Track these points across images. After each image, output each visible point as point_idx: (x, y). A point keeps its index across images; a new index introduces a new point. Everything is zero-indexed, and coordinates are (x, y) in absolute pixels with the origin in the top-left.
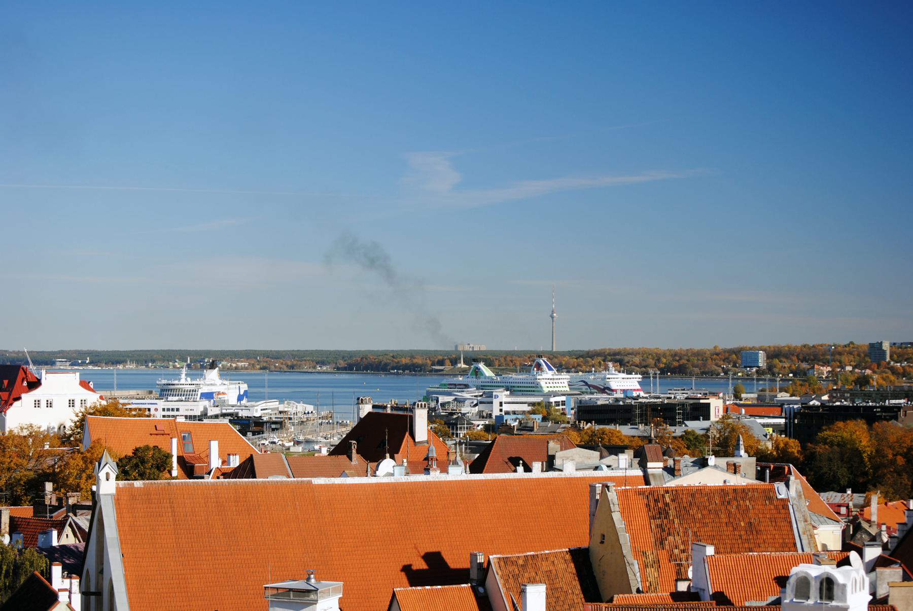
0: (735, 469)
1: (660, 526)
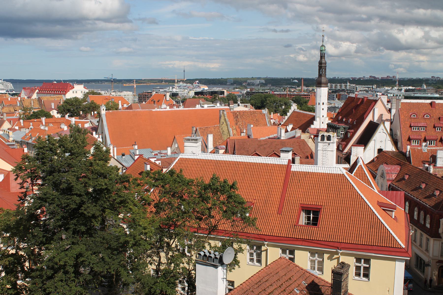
0: (246, 106)
1: (236, 120)
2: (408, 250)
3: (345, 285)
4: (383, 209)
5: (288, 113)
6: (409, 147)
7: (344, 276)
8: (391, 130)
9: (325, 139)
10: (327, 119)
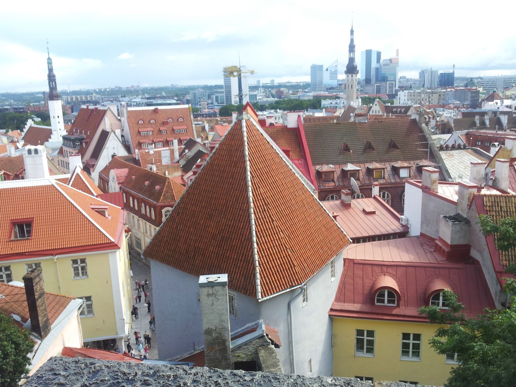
2: (118, 243)
3: (38, 288)
4: (96, 211)
5: (24, 129)
6: (137, 151)
7: (37, 280)
8: (122, 136)
9: (33, 152)
10: (65, 131)
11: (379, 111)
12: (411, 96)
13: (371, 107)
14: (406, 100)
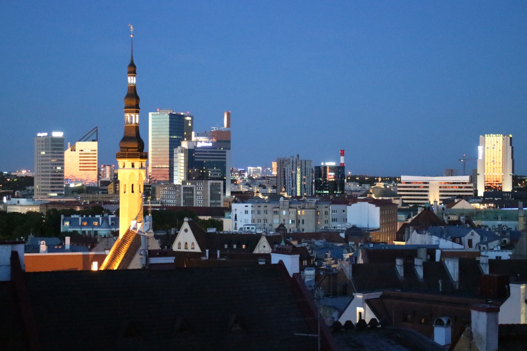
11: (193, 244)
12: (259, 213)
13: (176, 234)
14: (250, 223)
